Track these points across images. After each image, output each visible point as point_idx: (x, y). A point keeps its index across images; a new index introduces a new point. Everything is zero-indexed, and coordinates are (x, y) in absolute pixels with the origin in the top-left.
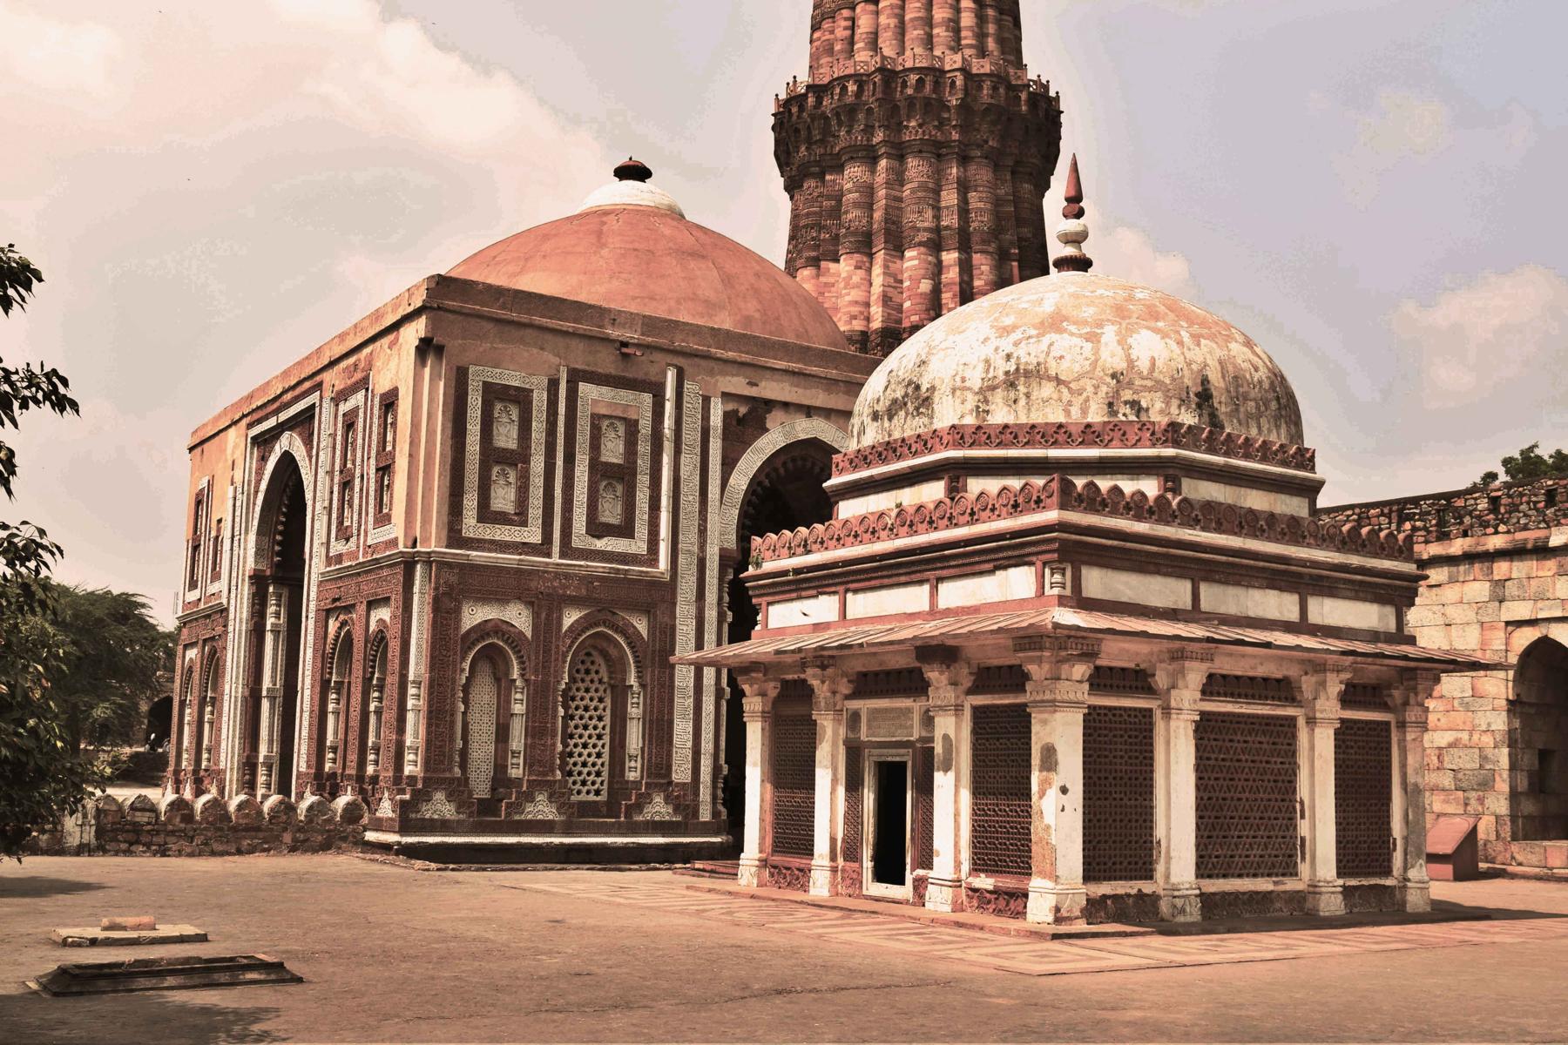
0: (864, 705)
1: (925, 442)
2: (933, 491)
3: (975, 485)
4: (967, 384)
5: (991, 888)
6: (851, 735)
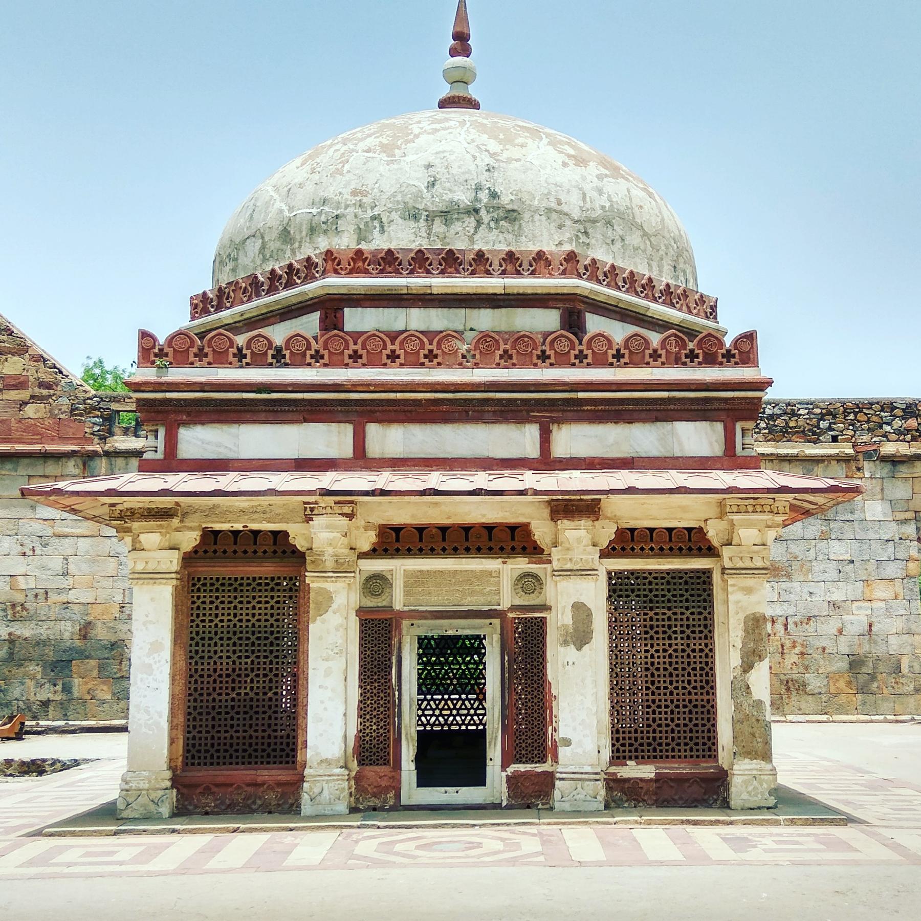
0: (398, 568)
1: (512, 262)
2: (547, 320)
3: (594, 324)
4: (565, 208)
5: (652, 776)
6: (370, 602)
